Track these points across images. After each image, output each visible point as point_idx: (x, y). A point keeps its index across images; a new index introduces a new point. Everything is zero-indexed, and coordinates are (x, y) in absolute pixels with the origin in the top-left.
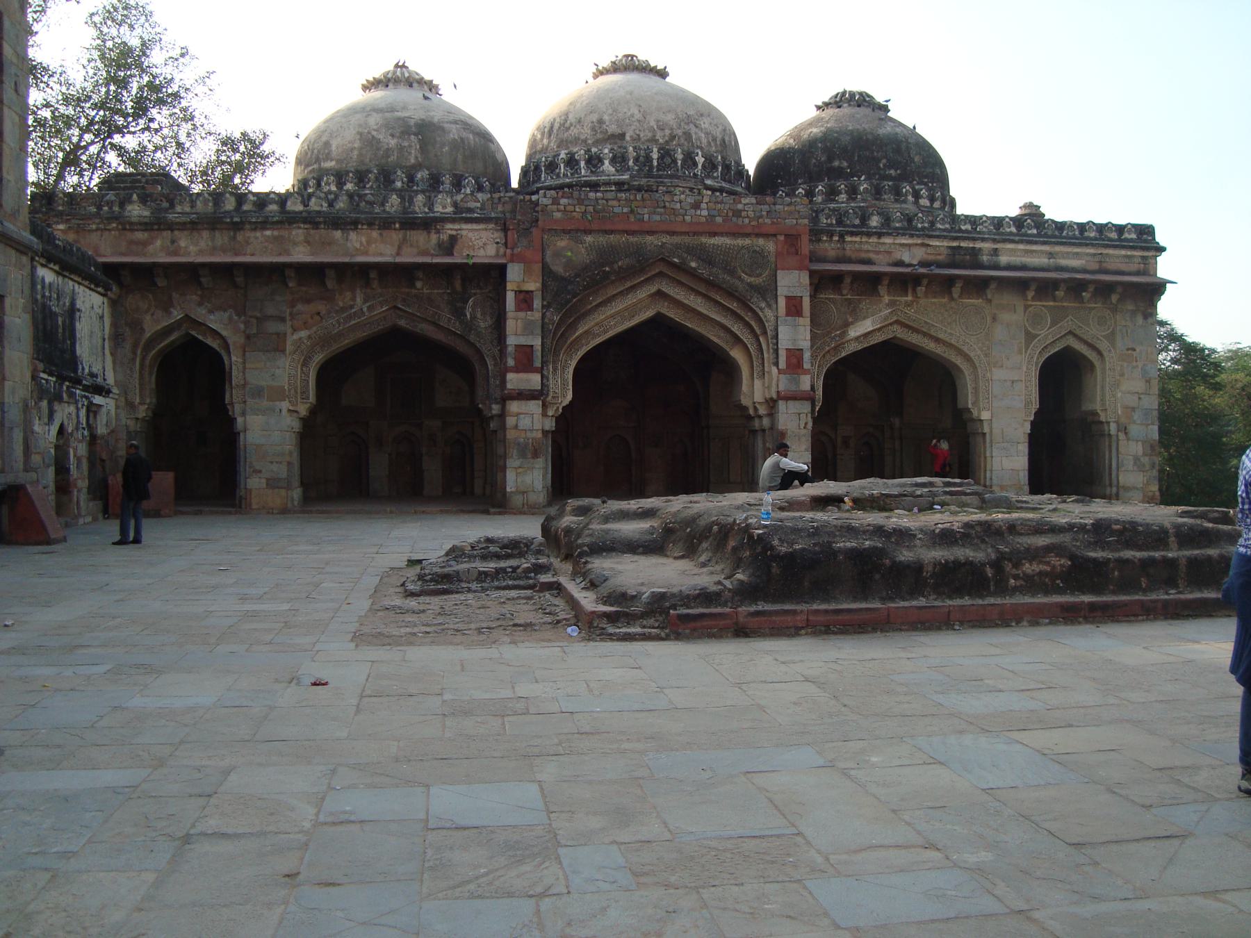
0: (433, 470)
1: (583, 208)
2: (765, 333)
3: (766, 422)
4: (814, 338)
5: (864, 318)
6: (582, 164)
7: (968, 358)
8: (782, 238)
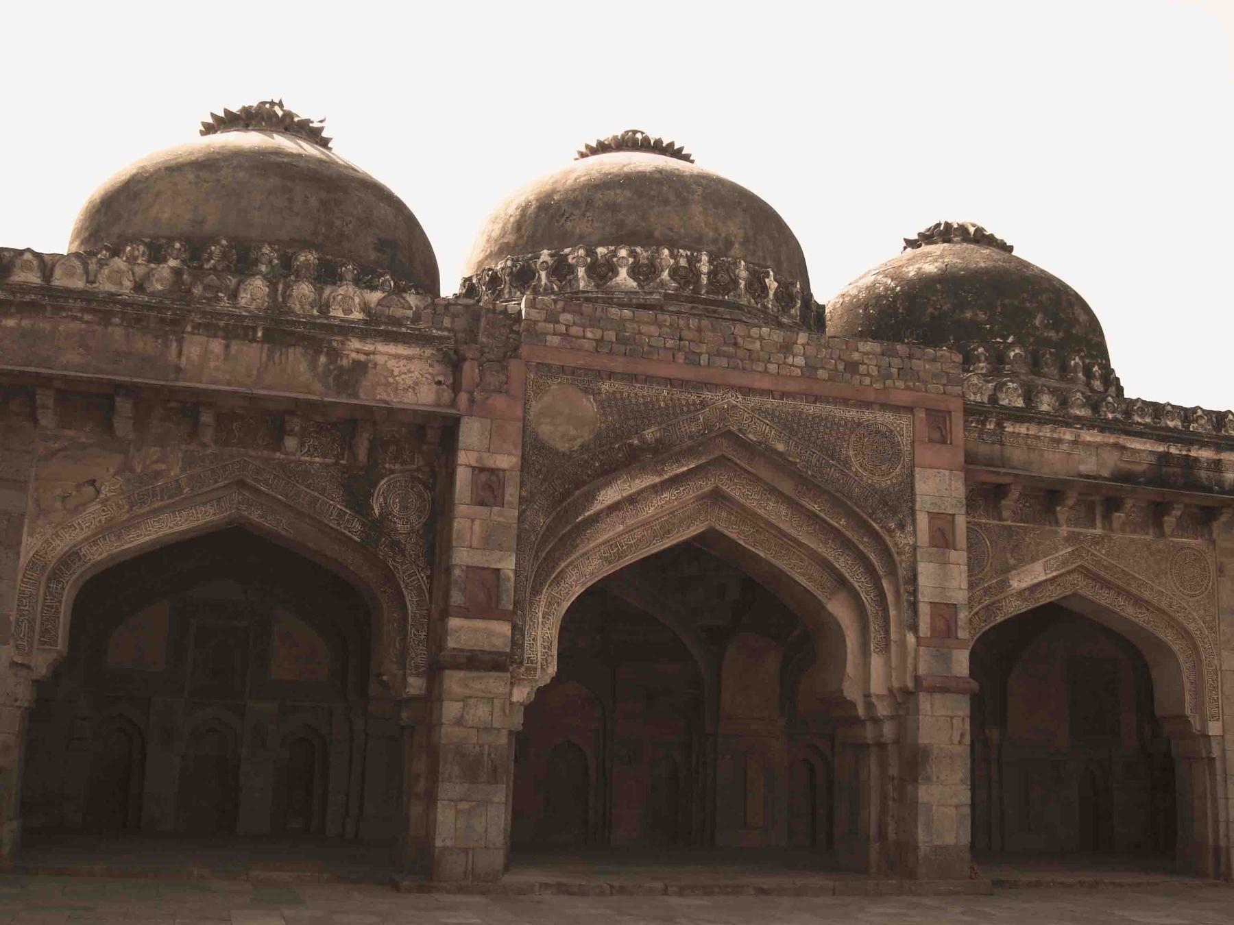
1: (599, 334)
4: (971, 586)
5: (1033, 560)
6: (581, 272)
7: (1185, 634)
8: (921, 414)
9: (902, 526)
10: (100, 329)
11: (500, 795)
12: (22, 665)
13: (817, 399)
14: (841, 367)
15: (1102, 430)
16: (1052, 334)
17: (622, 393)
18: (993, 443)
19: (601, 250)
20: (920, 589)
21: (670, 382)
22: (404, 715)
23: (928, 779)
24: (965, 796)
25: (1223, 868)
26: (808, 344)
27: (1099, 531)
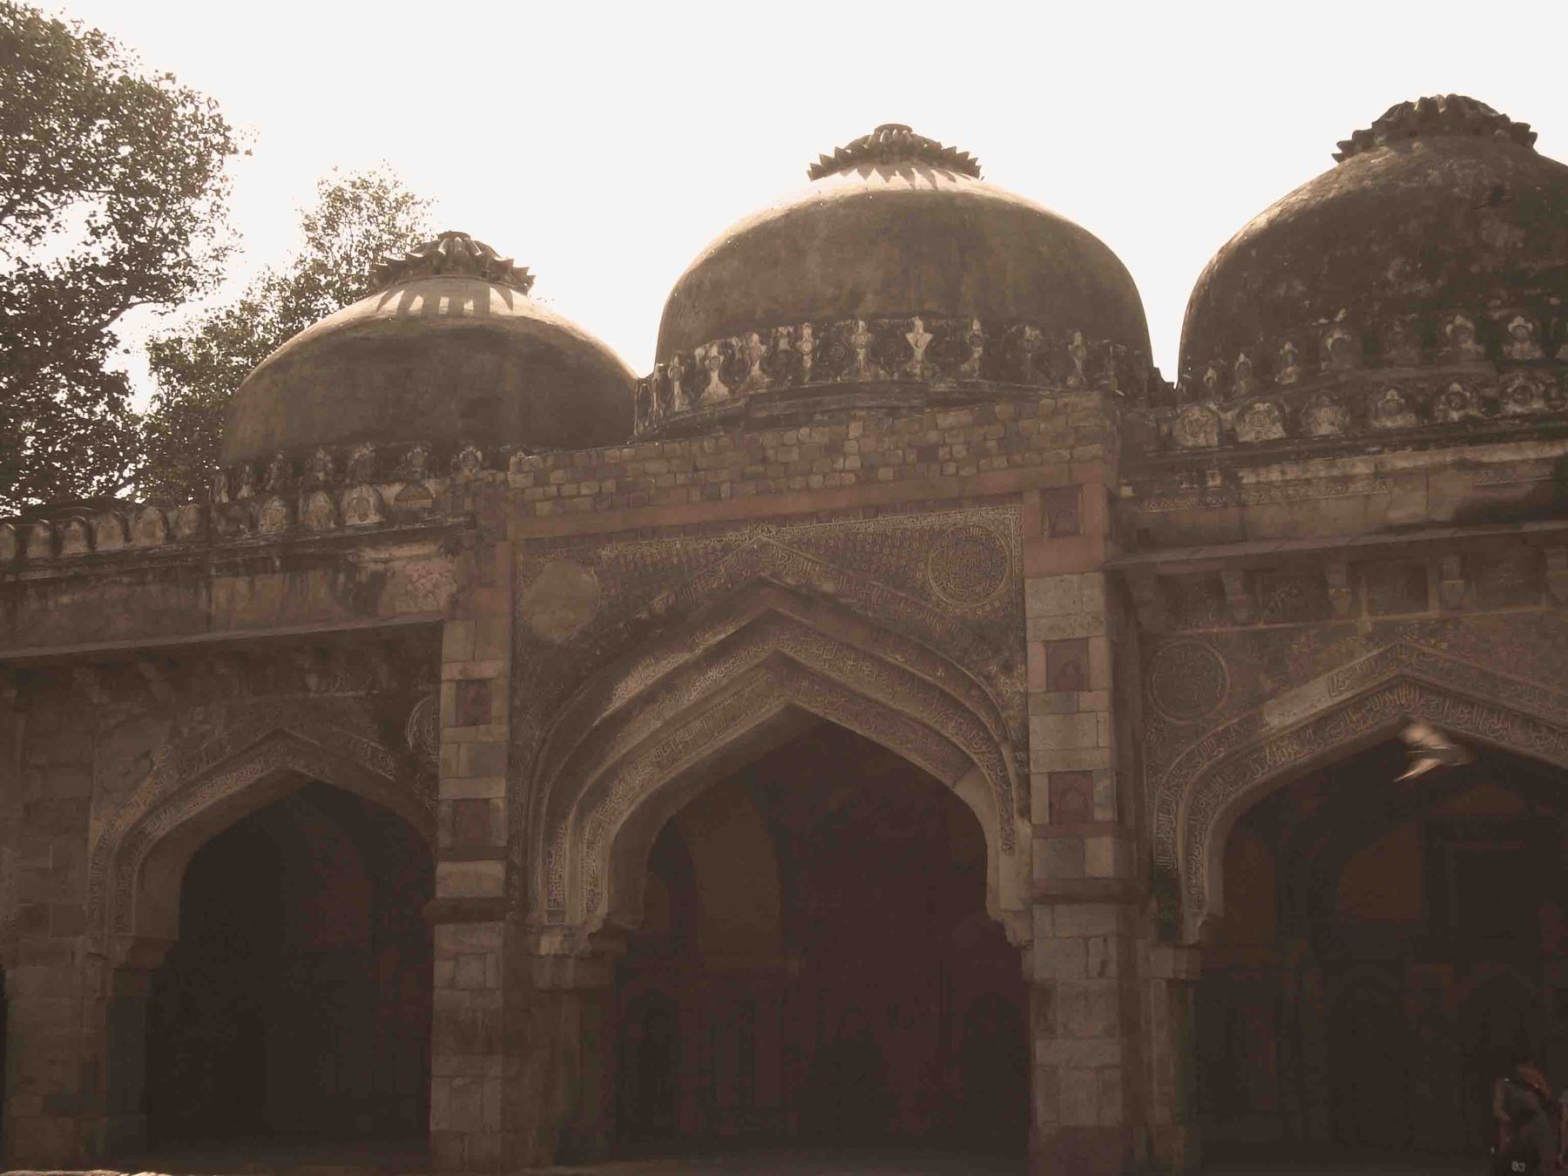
5: (1306, 680)
8: (1034, 499)
9: (1007, 668)
10: (139, 589)
13: (878, 510)
14: (912, 457)
15: (1442, 444)
16: (1422, 287)
17: (625, 556)
18: (1225, 506)
20: (1032, 756)
21: (685, 529)
26: (863, 436)
27: (1433, 613)
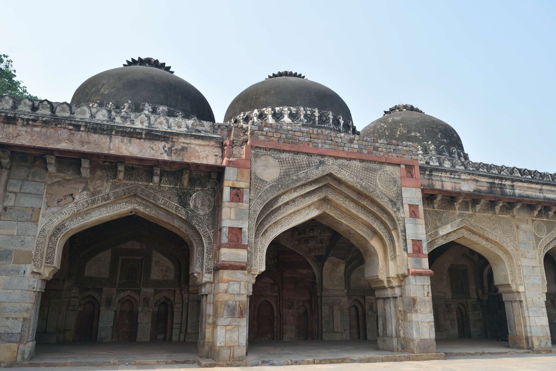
0: (145, 322)
1: (279, 135)
2: (396, 229)
3: (397, 291)
5: (447, 223)
7: (506, 252)
8: (403, 166)
9: (398, 210)
11: (244, 323)
12: (37, 273)
15: (469, 174)
16: (445, 140)
19: (277, 109)
20: (407, 234)
22: (203, 290)
23: (416, 311)
24: (431, 318)
25: (530, 345)
